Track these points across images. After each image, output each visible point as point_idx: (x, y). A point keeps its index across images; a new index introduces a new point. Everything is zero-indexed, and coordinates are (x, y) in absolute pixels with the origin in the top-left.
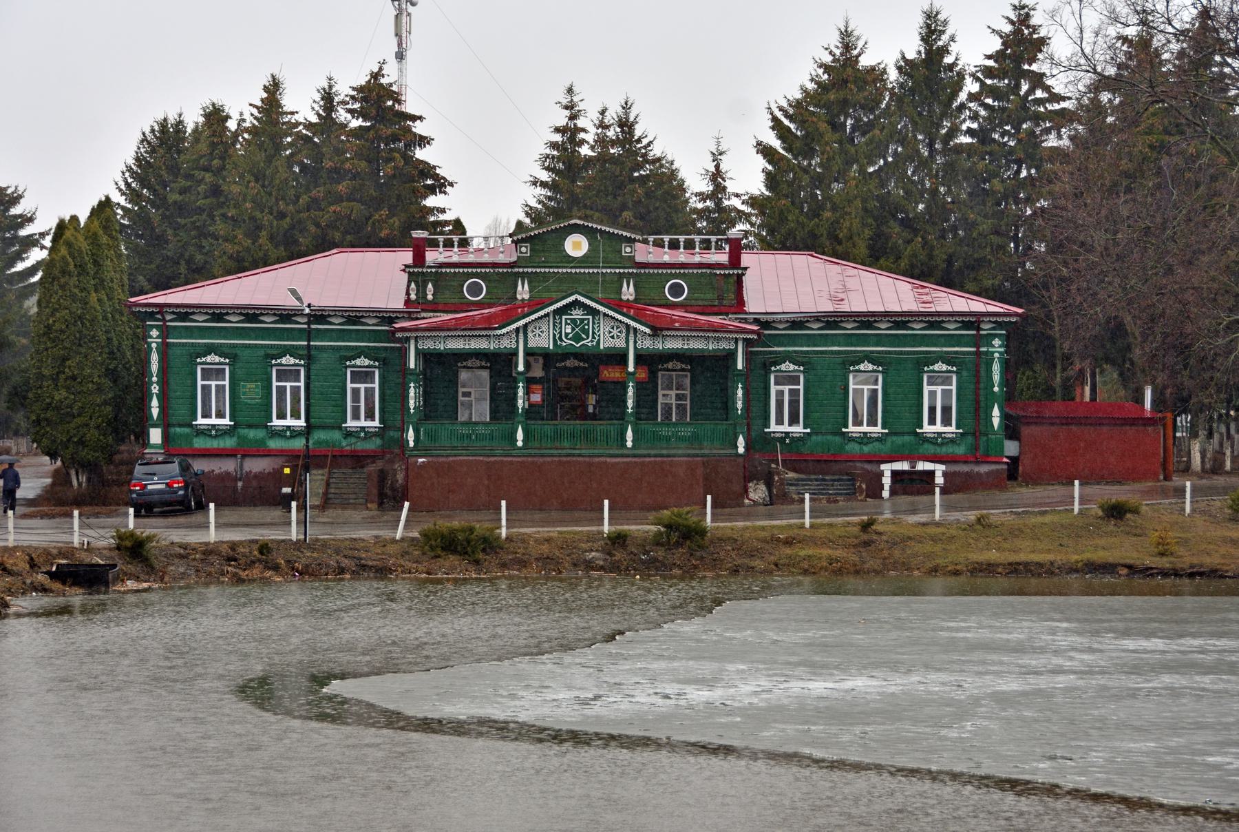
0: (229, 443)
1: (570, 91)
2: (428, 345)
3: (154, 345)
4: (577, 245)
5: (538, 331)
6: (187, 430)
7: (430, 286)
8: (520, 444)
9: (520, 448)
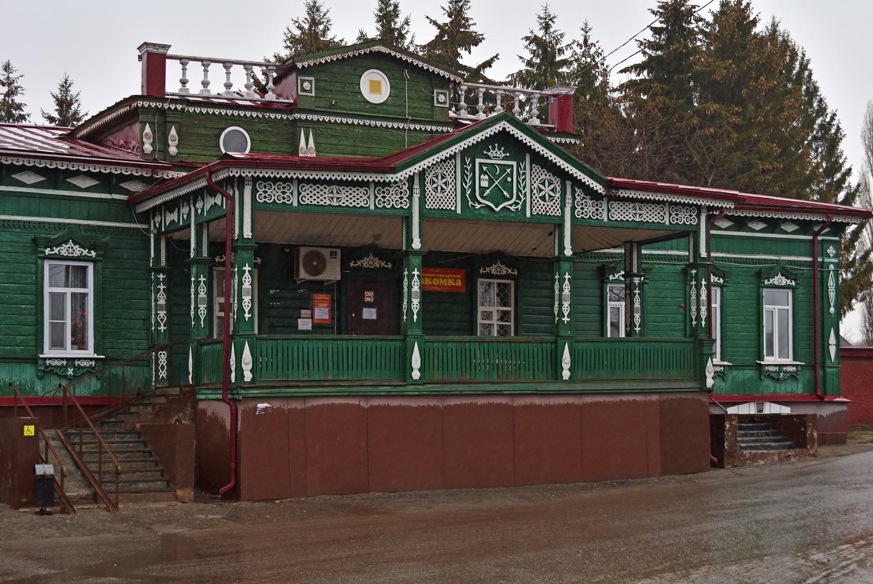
1: (7, 68)
2: (273, 195)
4: (375, 87)
5: (440, 182)
7: (173, 132)
8: (416, 375)
9: (416, 383)
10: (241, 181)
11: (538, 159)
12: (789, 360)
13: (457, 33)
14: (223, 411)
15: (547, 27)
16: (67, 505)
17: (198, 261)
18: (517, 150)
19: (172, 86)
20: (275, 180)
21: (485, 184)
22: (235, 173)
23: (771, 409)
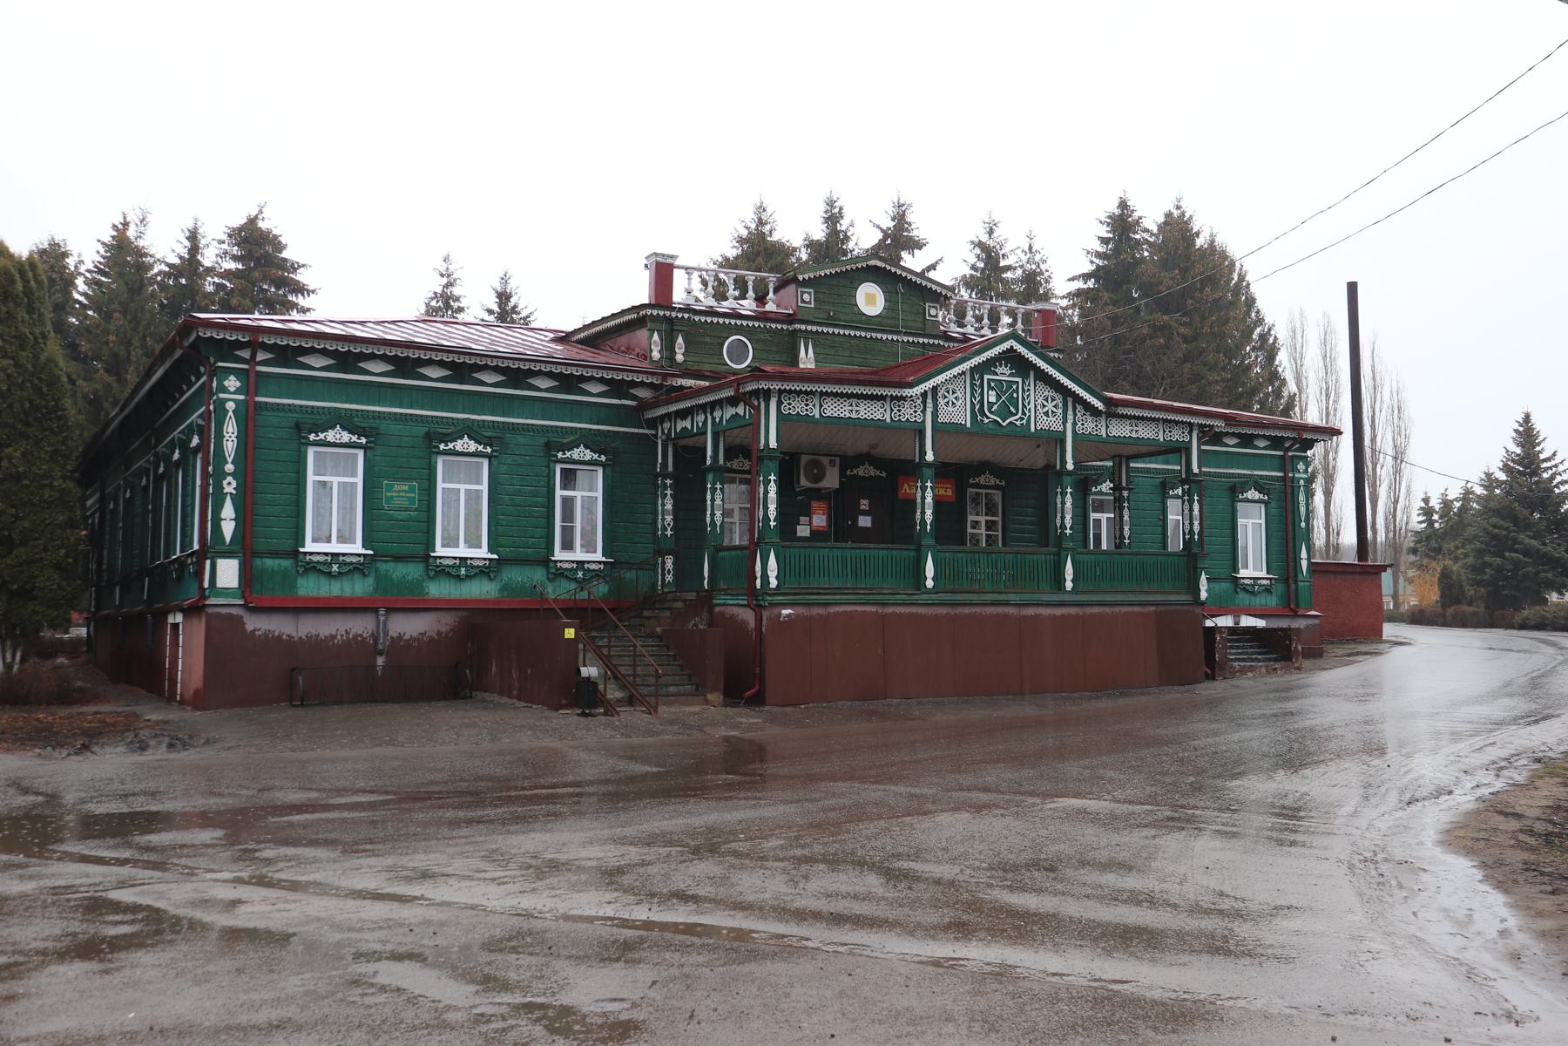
0: (358, 588)
1: (446, 260)
2: (797, 407)
3: (230, 406)
4: (871, 299)
5: (951, 397)
6: (286, 563)
7: (680, 340)
8: (930, 583)
9: (929, 592)
10: (767, 394)
11: (1043, 377)
12: (1263, 574)
13: (899, 238)
14: (748, 616)
15: (991, 232)
16: (610, 710)
17: (715, 468)
18: (1021, 366)
19: (679, 296)
20: (798, 393)
21: (993, 399)
22: (763, 385)
23: (1247, 621)
